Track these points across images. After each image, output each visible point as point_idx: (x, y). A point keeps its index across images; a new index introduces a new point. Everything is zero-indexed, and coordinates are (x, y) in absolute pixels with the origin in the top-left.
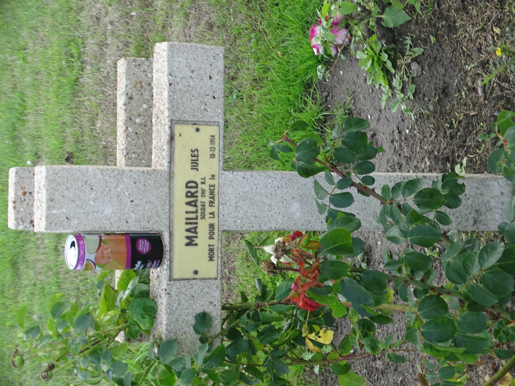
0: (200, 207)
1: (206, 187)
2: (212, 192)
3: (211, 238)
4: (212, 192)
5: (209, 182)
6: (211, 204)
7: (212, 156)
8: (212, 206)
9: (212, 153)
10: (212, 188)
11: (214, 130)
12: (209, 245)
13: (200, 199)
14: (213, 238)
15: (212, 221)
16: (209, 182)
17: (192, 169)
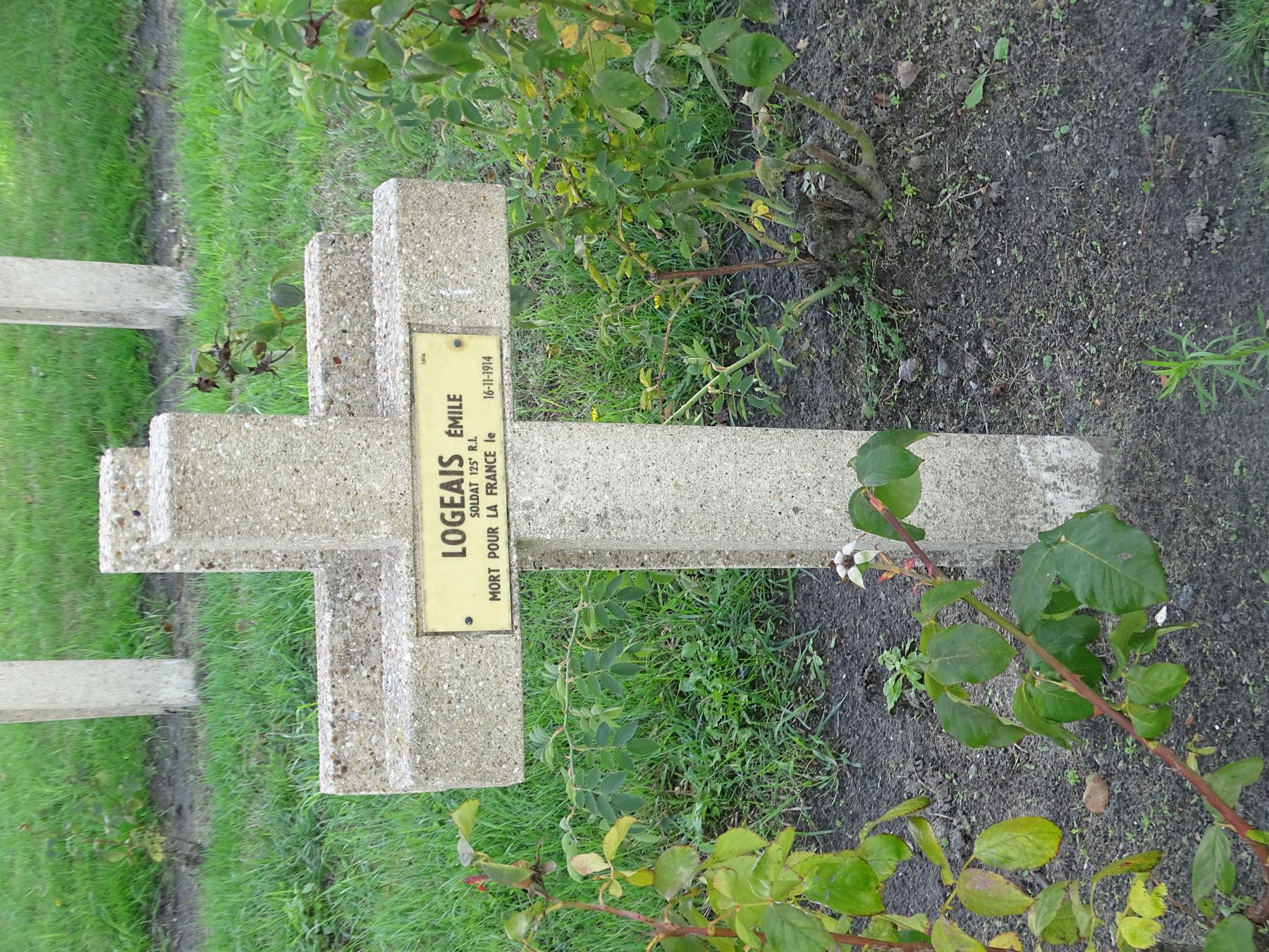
0: (467, 494)
1: (478, 456)
2: (490, 468)
3: (493, 555)
4: (490, 468)
5: (483, 447)
6: (490, 489)
7: (489, 394)
8: (492, 493)
9: (486, 388)
10: (490, 459)
11: (488, 346)
12: (490, 571)
13: (468, 478)
14: (496, 557)
15: (493, 523)
16: (483, 447)
17: (449, 433)
